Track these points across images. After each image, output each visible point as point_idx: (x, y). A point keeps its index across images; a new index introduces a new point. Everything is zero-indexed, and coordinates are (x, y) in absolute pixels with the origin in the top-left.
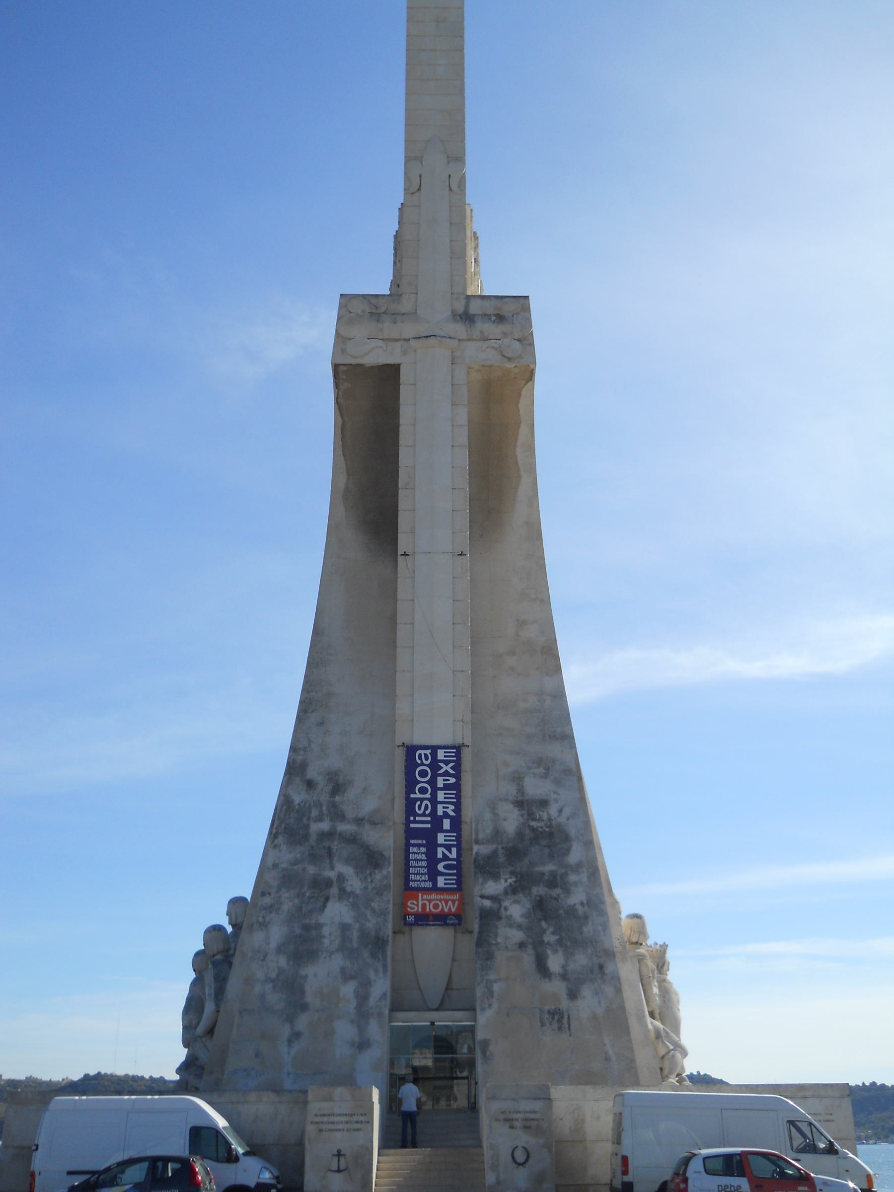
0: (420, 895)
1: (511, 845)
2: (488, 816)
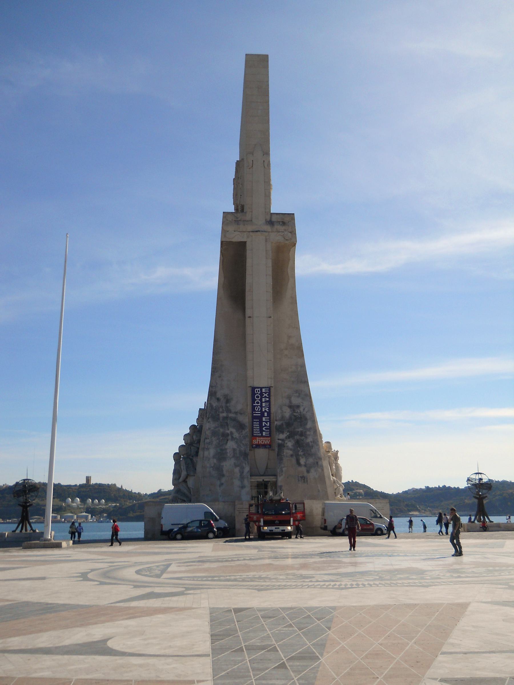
0: (257, 438)
1: (288, 422)
2: (279, 411)
